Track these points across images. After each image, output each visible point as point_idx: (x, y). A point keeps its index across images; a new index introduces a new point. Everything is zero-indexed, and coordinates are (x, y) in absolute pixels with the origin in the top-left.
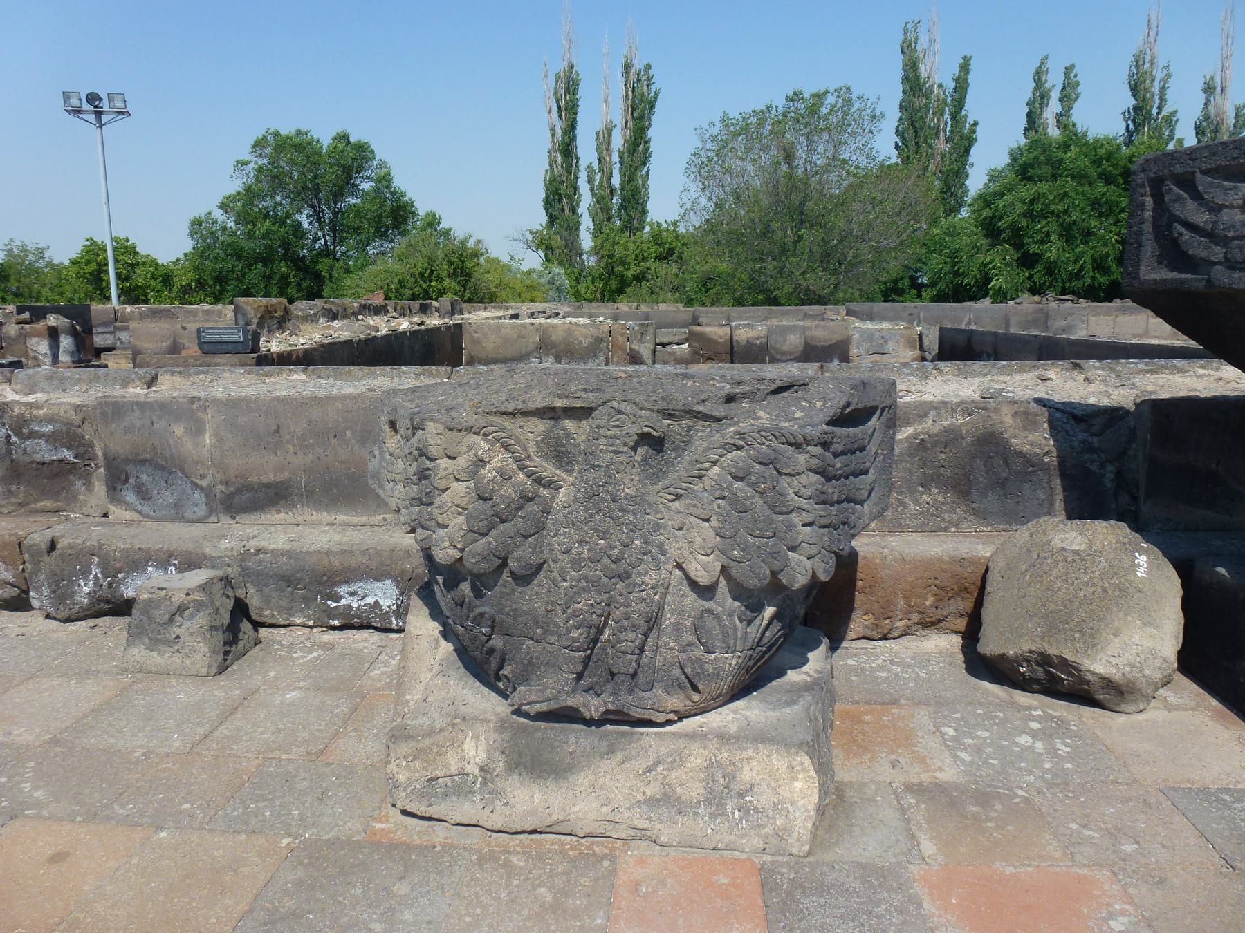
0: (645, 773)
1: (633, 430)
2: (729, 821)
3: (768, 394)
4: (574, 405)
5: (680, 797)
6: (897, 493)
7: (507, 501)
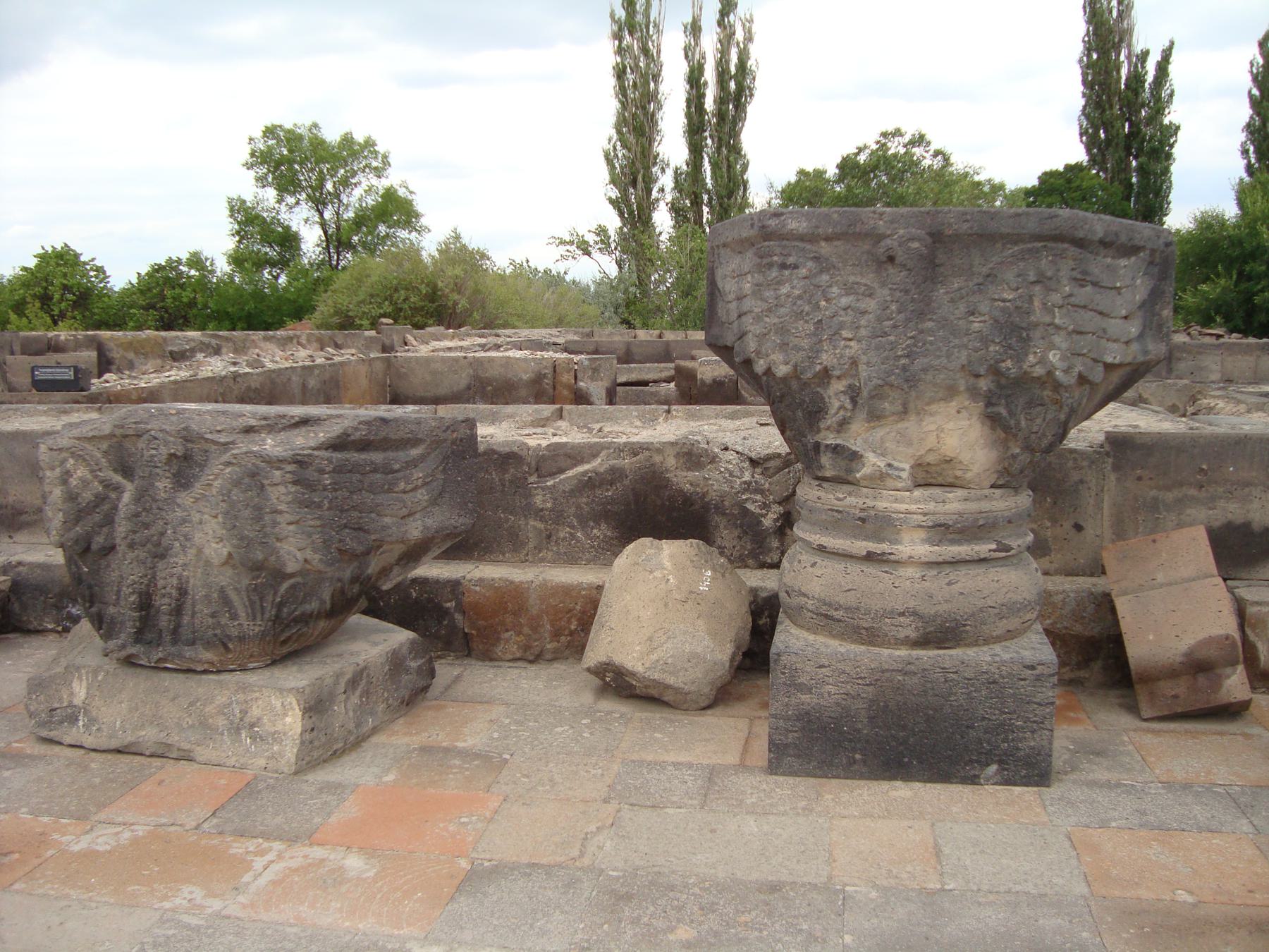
1: (164, 451)
6: (568, 526)
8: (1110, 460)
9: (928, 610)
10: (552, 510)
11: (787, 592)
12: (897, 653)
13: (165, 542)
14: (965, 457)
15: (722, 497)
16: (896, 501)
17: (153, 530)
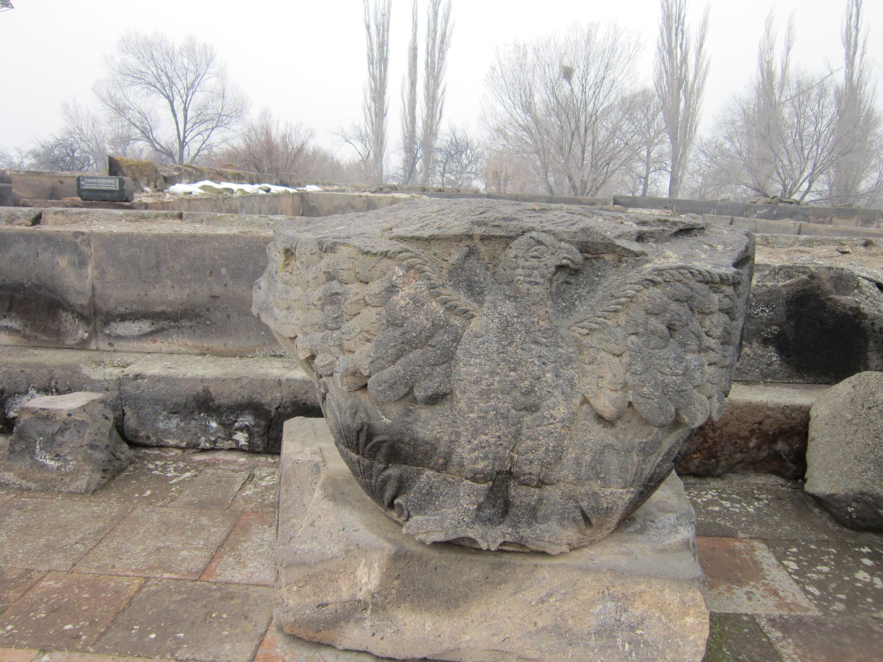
0: (537, 604)
1: (552, 261)
2: (619, 654)
3: (671, 235)
4: (492, 234)
5: (571, 629)
7: (419, 328)
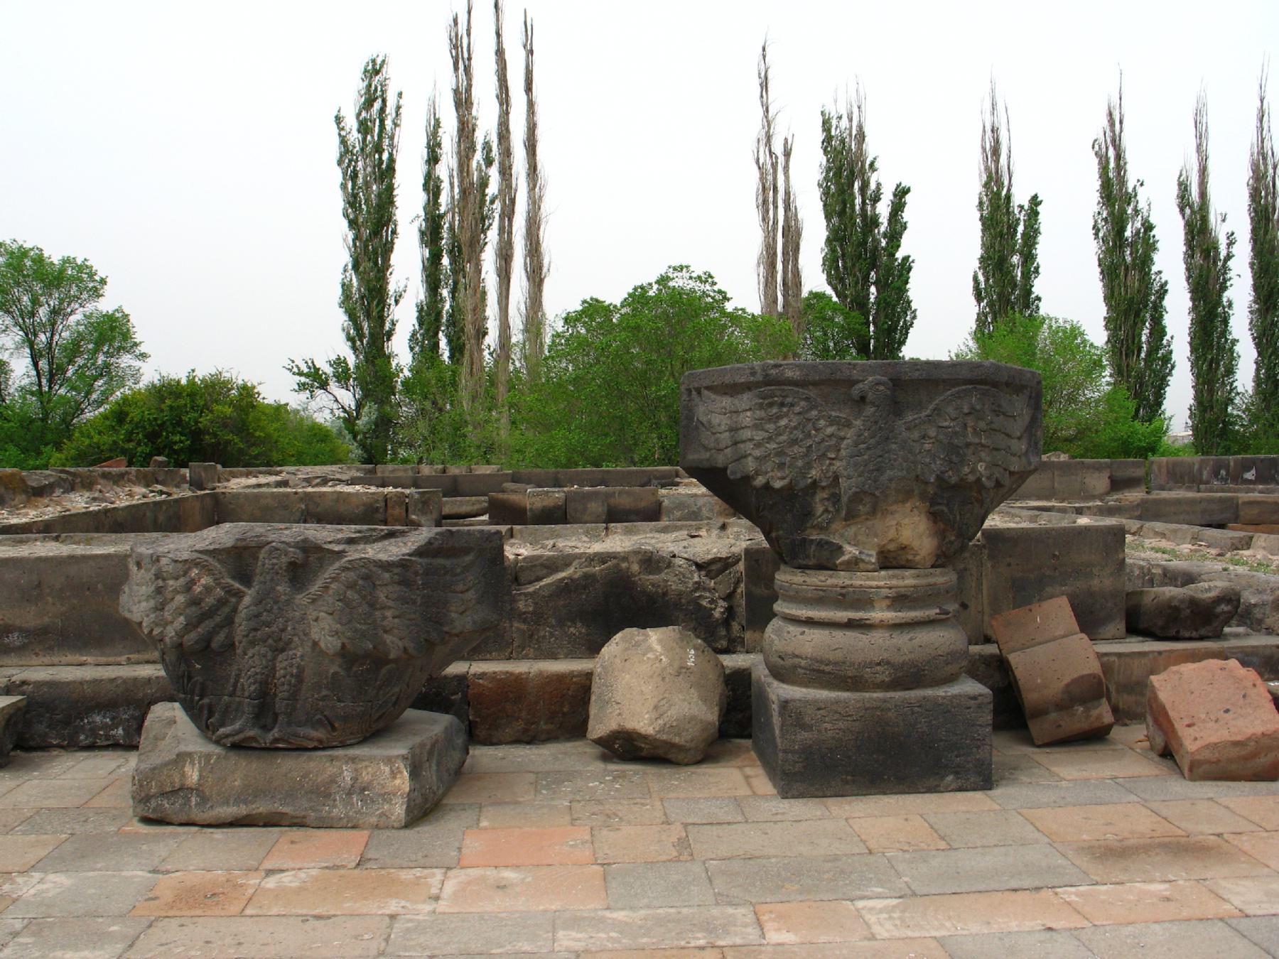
1: (284, 560)
8: (986, 551)
9: (898, 659)
10: (533, 613)
11: (780, 657)
12: (875, 695)
13: (285, 636)
14: (916, 544)
15: (680, 594)
16: (868, 579)
17: (274, 628)
